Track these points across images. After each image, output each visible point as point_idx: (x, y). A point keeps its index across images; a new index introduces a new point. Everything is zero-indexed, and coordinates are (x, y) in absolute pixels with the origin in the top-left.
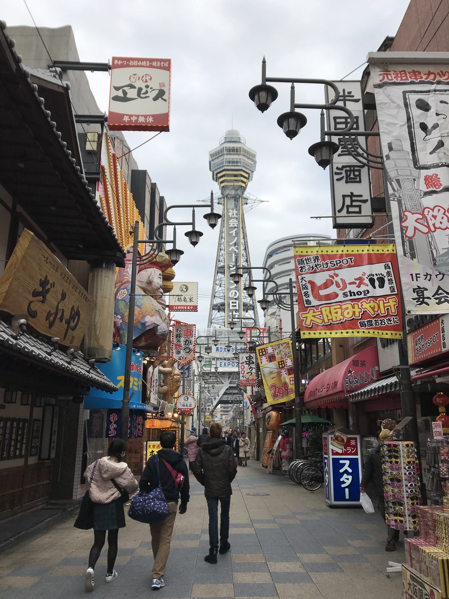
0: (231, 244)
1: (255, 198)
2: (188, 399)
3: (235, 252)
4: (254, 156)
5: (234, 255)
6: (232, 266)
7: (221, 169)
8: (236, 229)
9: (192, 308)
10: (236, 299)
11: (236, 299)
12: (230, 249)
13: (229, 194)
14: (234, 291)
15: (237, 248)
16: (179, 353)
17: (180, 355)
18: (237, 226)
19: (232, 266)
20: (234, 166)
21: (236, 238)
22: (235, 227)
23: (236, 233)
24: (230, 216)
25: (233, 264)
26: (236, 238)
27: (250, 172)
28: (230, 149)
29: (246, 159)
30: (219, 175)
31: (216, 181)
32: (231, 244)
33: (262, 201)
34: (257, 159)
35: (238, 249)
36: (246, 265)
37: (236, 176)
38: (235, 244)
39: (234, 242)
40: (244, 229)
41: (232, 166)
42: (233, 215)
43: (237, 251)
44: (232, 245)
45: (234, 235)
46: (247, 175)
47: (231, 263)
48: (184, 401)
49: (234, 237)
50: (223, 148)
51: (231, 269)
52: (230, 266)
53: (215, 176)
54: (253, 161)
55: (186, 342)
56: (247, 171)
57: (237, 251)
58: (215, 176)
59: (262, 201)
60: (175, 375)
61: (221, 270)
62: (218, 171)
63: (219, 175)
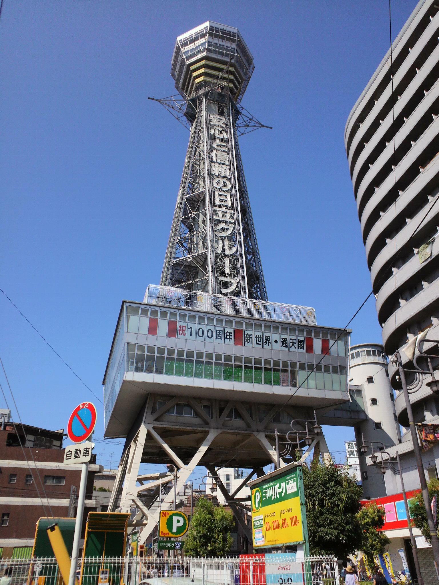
33: (263, 126)
59: (263, 126)
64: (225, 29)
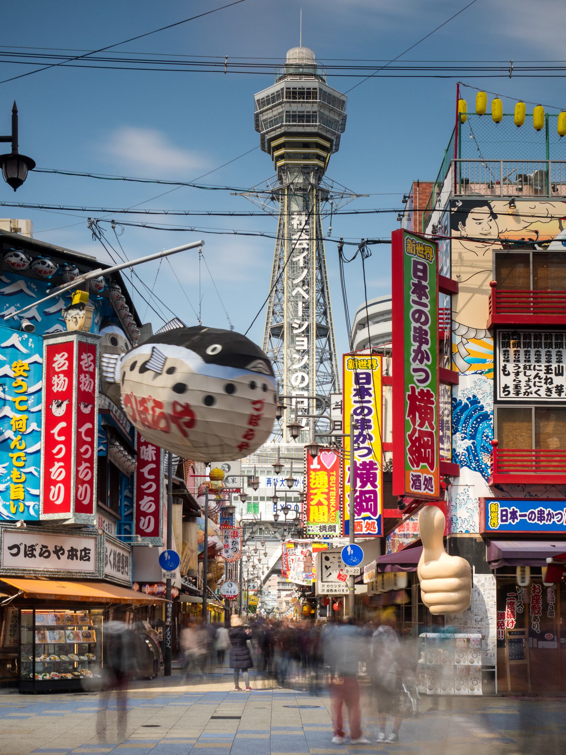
0: (295, 282)
1: (342, 190)
2: (232, 585)
3: (303, 297)
4: (342, 104)
5: (300, 304)
6: (297, 326)
7: (278, 132)
8: (305, 253)
9: (234, 490)
10: (303, 389)
11: (303, 389)
12: (294, 293)
13: (292, 183)
14: (300, 374)
15: (307, 291)
16: (227, 552)
17: (228, 554)
18: (306, 247)
19: (297, 326)
20: (303, 126)
21: (306, 271)
22: (304, 249)
23: (305, 262)
24: (295, 227)
25: (299, 322)
26: (306, 271)
27: (333, 138)
28: (294, 93)
29: (327, 113)
30: (273, 144)
31: (269, 153)
32: (295, 282)
34: (348, 111)
35: (308, 293)
36: (324, 323)
37: (306, 145)
38: (303, 281)
39: (301, 278)
40: (321, 252)
41: (299, 126)
42: (301, 224)
43: (306, 296)
44: (297, 286)
45: (301, 264)
46: (328, 144)
47: (296, 321)
48: (228, 588)
49: (302, 268)
50: (282, 89)
51: (295, 332)
52: (294, 325)
53: (266, 145)
54: (340, 114)
55: (233, 542)
56: (328, 135)
57: (306, 296)
58: (266, 145)
60: (219, 562)
61: (276, 331)
62: (273, 134)
63: (273, 144)
64: (304, 86)
